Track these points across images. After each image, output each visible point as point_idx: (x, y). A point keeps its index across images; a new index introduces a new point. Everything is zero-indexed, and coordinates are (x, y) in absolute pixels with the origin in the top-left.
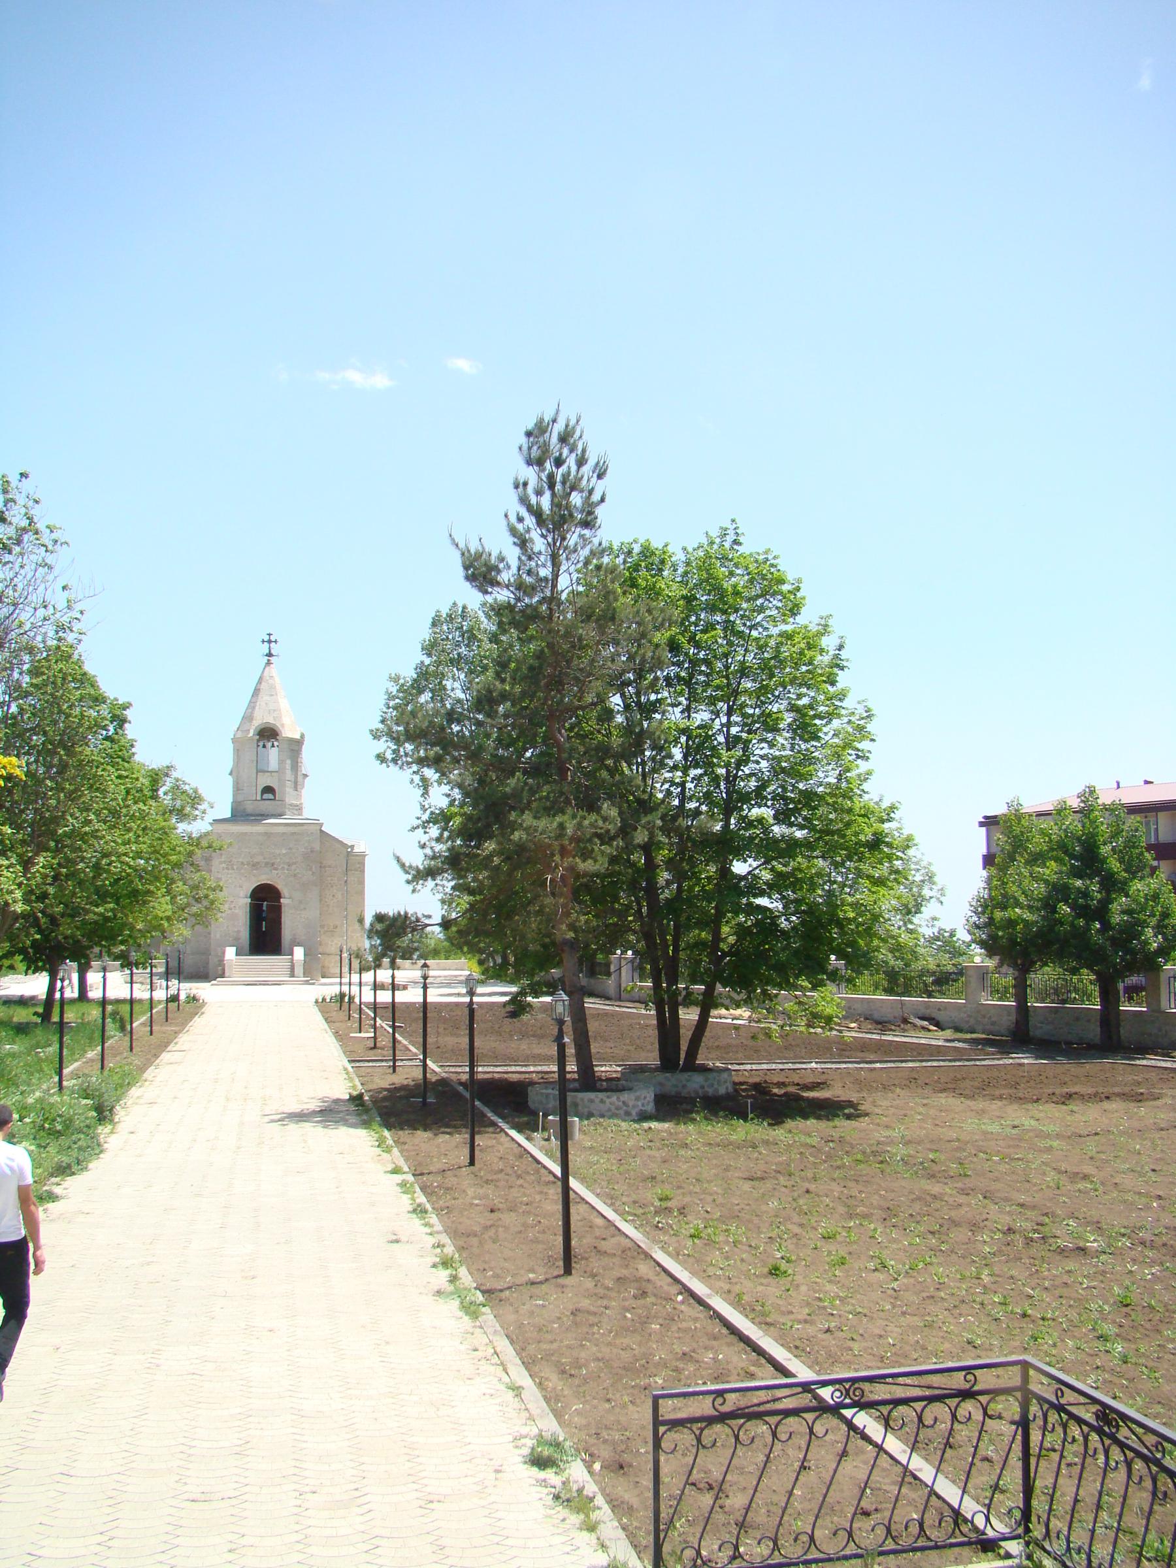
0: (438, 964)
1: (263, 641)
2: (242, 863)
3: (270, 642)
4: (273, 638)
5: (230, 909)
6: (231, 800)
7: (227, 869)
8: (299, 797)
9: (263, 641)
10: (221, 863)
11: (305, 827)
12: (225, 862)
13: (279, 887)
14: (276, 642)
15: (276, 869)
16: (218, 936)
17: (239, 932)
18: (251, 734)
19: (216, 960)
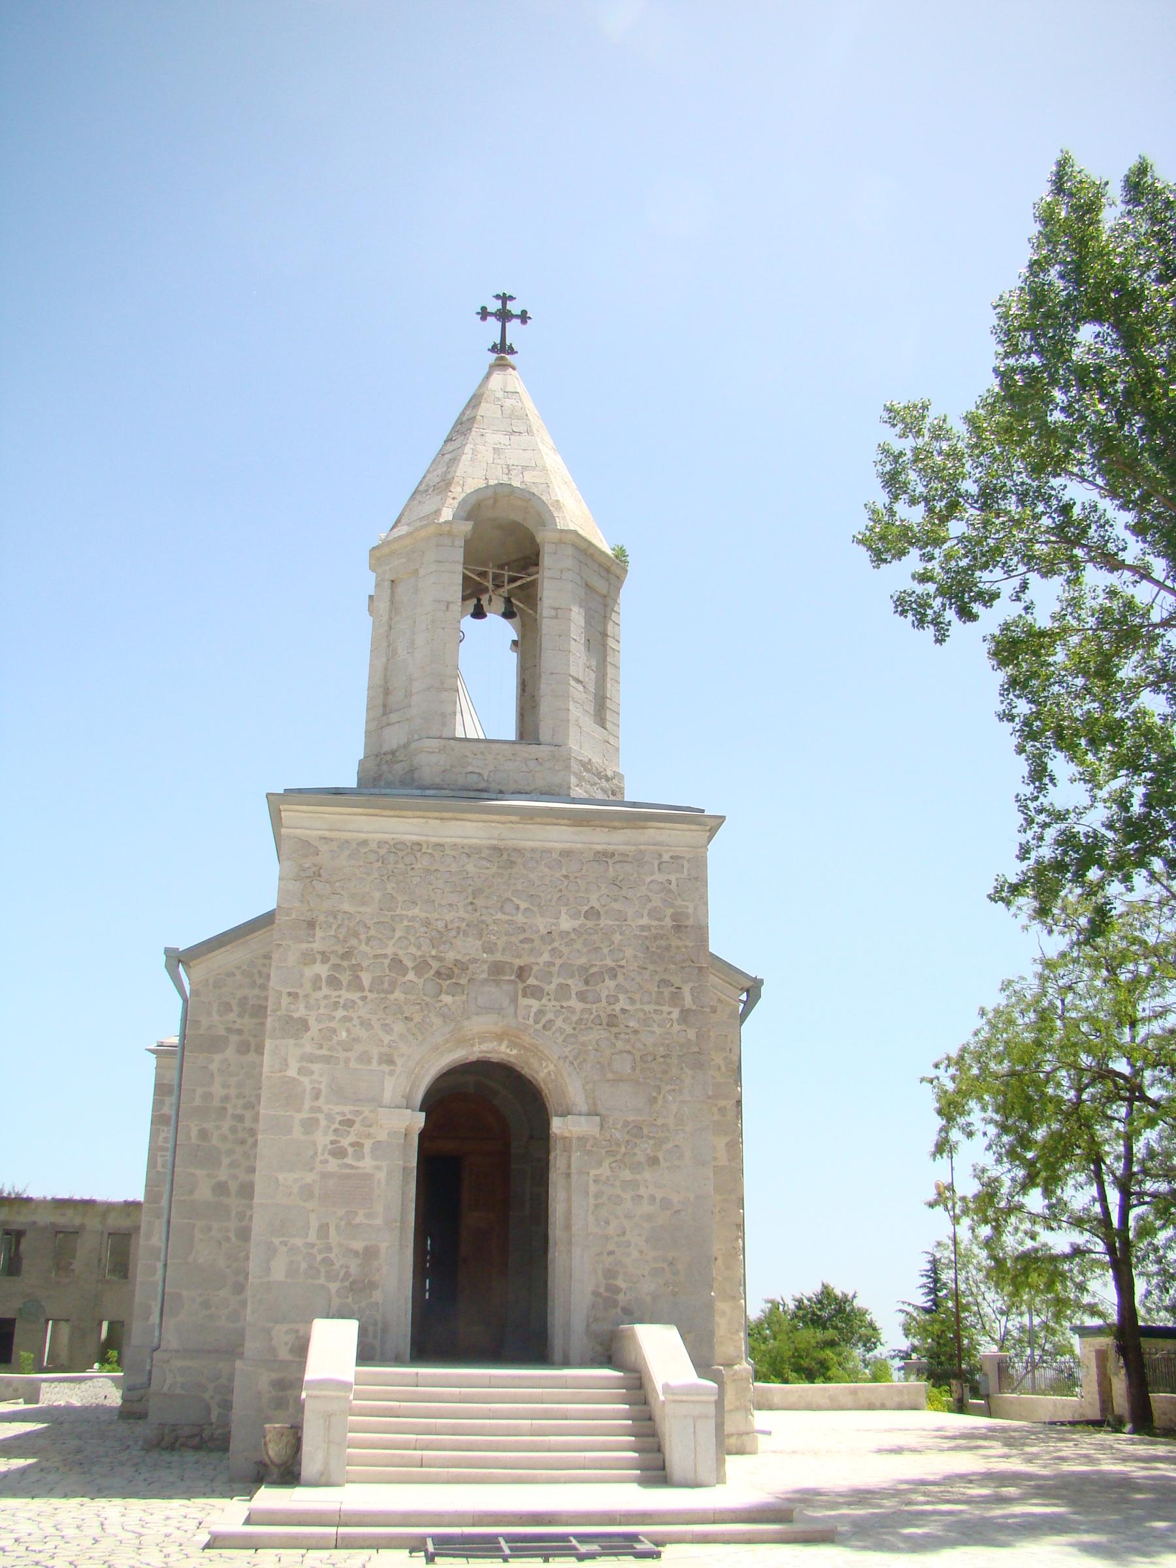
0: (854, 1392)
1: (484, 314)
2: (397, 963)
3: (504, 316)
4: (514, 307)
5: (339, 1153)
7: (333, 982)
8: (611, 749)
10: (308, 958)
11: (651, 833)
12: (325, 958)
14: (524, 317)
15: (535, 992)
16: (279, 1272)
17: (370, 1253)
18: (447, 514)
19: (264, 1379)
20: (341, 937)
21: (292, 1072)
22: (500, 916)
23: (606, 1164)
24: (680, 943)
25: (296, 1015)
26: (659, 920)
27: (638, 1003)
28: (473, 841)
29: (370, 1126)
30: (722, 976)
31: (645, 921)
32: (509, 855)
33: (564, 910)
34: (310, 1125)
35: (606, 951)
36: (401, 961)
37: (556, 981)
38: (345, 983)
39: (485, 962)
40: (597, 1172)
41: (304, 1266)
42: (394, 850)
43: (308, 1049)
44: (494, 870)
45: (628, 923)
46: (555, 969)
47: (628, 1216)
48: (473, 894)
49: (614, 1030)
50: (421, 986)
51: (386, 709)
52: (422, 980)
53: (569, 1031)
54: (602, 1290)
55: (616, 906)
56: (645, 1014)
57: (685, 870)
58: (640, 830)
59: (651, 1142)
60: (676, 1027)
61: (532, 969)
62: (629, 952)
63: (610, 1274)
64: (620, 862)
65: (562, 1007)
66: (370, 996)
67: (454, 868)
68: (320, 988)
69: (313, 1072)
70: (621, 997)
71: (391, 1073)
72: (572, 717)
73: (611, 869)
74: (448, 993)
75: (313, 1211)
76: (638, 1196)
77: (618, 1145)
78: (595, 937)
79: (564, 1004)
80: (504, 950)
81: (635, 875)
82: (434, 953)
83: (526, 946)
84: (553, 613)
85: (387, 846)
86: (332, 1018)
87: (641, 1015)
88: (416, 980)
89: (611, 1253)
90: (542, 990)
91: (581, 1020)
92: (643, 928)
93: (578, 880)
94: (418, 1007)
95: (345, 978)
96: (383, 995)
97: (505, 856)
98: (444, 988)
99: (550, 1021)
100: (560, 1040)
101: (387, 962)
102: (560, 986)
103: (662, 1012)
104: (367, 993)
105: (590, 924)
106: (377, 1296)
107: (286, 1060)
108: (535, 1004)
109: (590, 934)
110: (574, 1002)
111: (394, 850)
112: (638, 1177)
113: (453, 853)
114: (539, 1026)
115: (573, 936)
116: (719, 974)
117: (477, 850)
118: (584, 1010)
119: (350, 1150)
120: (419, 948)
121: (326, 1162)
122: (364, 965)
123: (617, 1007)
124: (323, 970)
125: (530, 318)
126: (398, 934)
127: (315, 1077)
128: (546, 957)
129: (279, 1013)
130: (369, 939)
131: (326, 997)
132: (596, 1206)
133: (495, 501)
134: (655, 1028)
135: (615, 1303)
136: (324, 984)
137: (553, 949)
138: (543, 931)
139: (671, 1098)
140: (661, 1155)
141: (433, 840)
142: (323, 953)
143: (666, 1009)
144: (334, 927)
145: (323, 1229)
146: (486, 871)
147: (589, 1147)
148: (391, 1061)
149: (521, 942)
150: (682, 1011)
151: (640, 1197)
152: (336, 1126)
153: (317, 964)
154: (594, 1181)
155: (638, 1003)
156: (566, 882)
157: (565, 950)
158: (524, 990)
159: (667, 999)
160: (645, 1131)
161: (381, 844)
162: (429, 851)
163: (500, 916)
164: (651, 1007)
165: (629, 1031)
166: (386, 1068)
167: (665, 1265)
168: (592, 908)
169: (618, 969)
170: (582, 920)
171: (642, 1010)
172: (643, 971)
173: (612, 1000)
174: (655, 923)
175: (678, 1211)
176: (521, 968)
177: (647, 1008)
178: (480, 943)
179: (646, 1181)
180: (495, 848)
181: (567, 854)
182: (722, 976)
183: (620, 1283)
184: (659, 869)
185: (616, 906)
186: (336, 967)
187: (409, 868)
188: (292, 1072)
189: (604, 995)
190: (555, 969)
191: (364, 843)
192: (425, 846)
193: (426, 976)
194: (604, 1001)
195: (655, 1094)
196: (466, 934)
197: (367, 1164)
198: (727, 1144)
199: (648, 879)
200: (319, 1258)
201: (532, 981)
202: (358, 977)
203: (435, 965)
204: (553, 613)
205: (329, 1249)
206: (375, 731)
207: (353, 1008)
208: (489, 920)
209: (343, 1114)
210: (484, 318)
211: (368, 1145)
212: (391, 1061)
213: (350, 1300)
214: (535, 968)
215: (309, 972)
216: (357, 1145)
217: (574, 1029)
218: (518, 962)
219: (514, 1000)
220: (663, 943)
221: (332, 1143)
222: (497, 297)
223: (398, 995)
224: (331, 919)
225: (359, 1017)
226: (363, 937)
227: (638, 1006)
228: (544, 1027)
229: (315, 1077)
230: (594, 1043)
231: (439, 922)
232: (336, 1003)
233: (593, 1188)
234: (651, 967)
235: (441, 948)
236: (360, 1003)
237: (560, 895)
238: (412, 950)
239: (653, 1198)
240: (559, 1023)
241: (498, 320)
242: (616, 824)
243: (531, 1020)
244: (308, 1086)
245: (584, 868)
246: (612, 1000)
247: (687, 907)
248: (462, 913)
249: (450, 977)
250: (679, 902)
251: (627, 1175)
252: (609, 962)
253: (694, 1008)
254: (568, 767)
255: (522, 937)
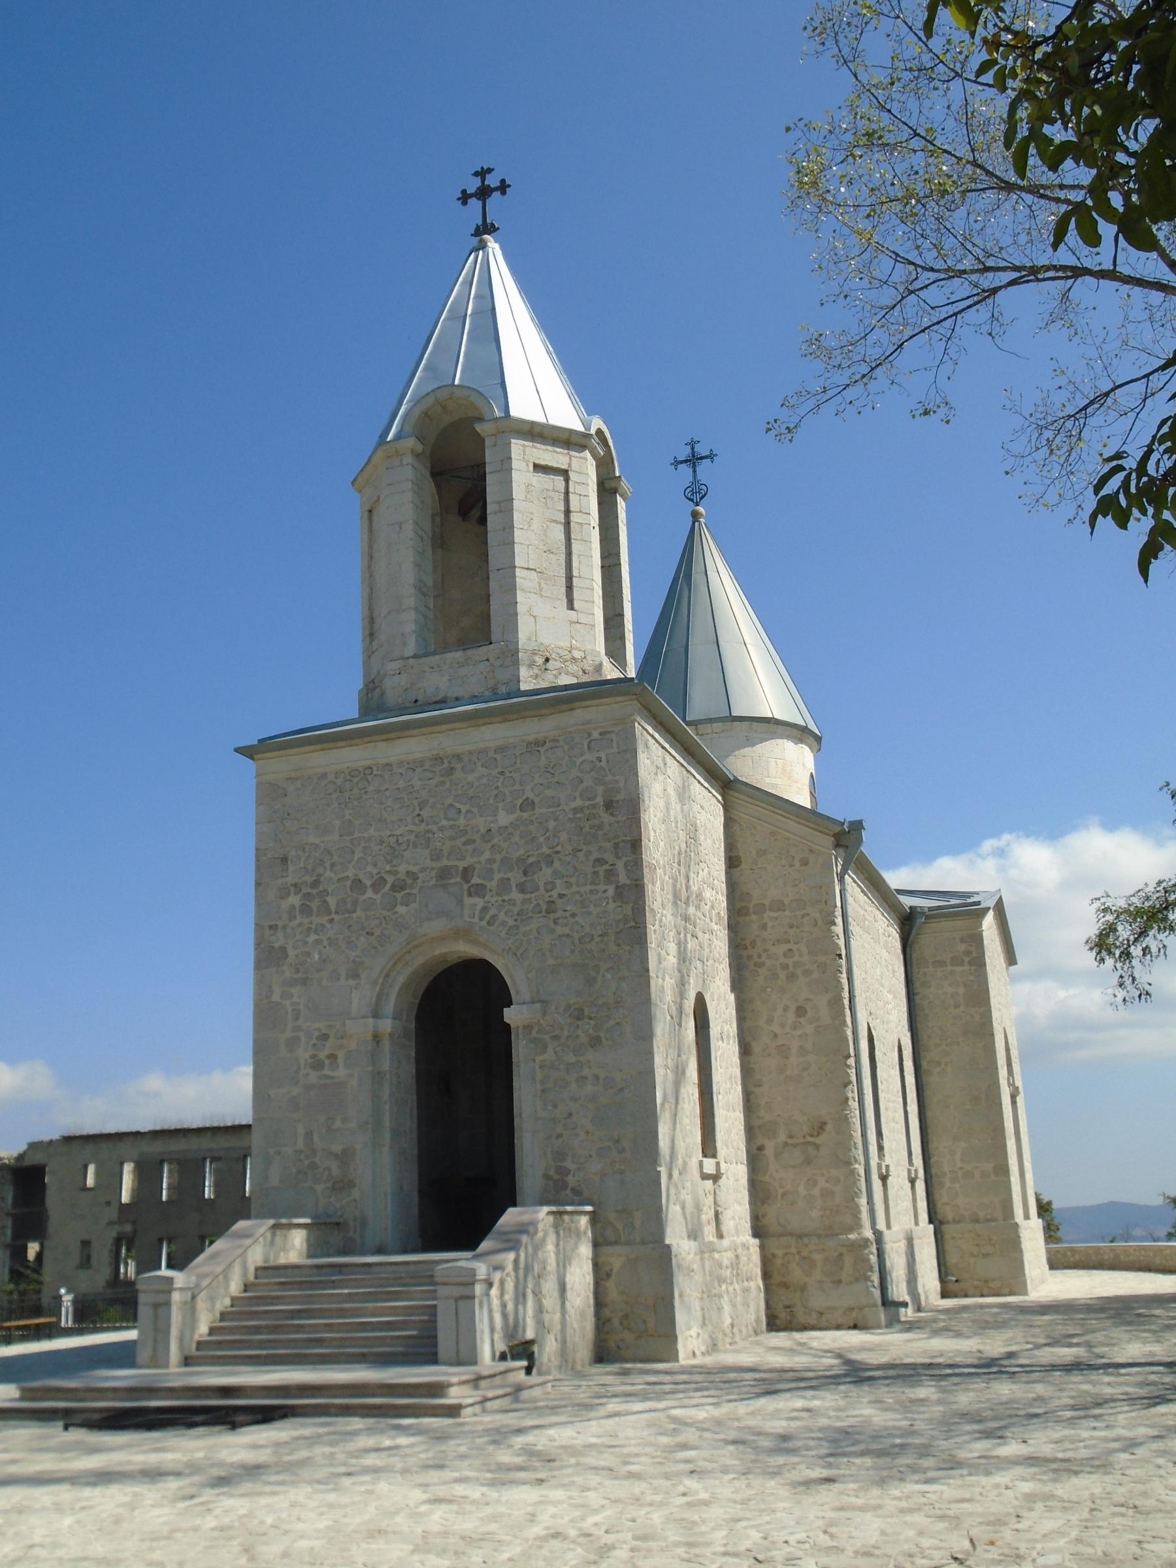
1: (465, 198)
2: (358, 884)
4: (492, 181)
5: (317, 1065)
6: (360, 684)
7: (306, 910)
9: (465, 198)
10: (284, 893)
13: (499, 963)
14: (503, 187)
15: (478, 891)
20: (310, 867)
21: (276, 997)
22: (444, 822)
23: (550, 1049)
24: (612, 819)
25: (277, 945)
26: (590, 799)
27: (574, 886)
28: (418, 755)
29: (342, 1038)
30: (812, 825)
31: (578, 803)
32: (449, 763)
33: (500, 805)
34: (292, 1044)
35: (542, 839)
36: (360, 881)
37: (497, 876)
38: (315, 909)
39: (433, 869)
40: (542, 1058)
41: (294, 1171)
42: (349, 778)
43: (288, 973)
44: (438, 779)
45: (561, 808)
46: (495, 866)
47: (575, 1100)
48: (419, 805)
49: (552, 916)
50: (378, 901)
51: (372, 635)
52: (379, 896)
53: (511, 922)
54: (552, 1173)
55: (549, 793)
56: (582, 896)
57: (615, 745)
58: (567, 713)
59: (593, 1022)
60: (612, 905)
61: (474, 869)
62: (564, 837)
63: (560, 1156)
64: (552, 748)
65: (504, 901)
66: (337, 918)
67: (401, 784)
68: (295, 917)
69: (292, 996)
70: (558, 882)
71: (356, 988)
72: (521, 609)
73: (543, 757)
74: (401, 904)
75: (299, 1121)
76: (582, 1077)
77: (562, 1029)
78: (532, 828)
79: (506, 898)
80: (449, 854)
81: (567, 758)
82: (388, 868)
83: (470, 848)
84: (496, 507)
85: (343, 775)
86: (306, 943)
87: (578, 897)
88: (375, 897)
89: (560, 1136)
90: (483, 886)
91: (522, 910)
92: (575, 810)
93: (513, 774)
94: (376, 922)
95: (315, 905)
96: (347, 915)
97: (446, 765)
98: (399, 900)
99: (493, 916)
100: (504, 933)
101: (348, 883)
102: (501, 880)
103: (598, 892)
104: (334, 916)
105: (525, 815)
106: (356, 1193)
107: (270, 986)
108: (479, 902)
109: (526, 825)
110: (515, 895)
111: (349, 778)
112: (582, 1059)
113: (400, 770)
114: (484, 923)
115: (510, 830)
116: (807, 823)
117: (421, 763)
118: (524, 901)
119: (327, 1062)
120: (375, 865)
121: (308, 1074)
122: (330, 890)
123: (555, 893)
124: (295, 900)
125: (509, 186)
126: (356, 858)
127: (295, 999)
128: (487, 855)
129: (263, 946)
130: (332, 865)
131: (300, 925)
132: (543, 1091)
133: (444, 408)
134: (592, 908)
135: (565, 1185)
136: (297, 912)
137: (493, 846)
138: (483, 830)
139: (609, 976)
140: (602, 1034)
141: (383, 761)
142: (295, 885)
143: (602, 887)
144: (303, 859)
145: (309, 1135)
146: (428, 782)
147: (534, 1034)
148: (356, 976)
149: (464, 844)
150: (617, 887)
151: (586, 1078)
152: (315, 1041)
153: (292, 895)
154: (540, 1067)
155: (574, 886)
156: (502, 778)
157: (504, 845)
158: (469, 890)
159: (602, 878)
160: (586, 1013)
161: (337, 774)
162: (379, 773)
163: (444, 822)
164: (589, 887)
165: (568, 914)
166: (352, 982)
167: (611, 1144)
168: (527, 799)
169: (554, 855)
170: (518, 813)
171: (578, 892)
172: (580, 854)
173: (550, 886)
174: (587, 803)
175: (622, 1089)
176: (465, 869)
177: (582, 890)
178: (427, 852)
179: (589, 1061)
180: (438, 759)
181: (501, 749)
182: (812, 825)
183: (569, 1164)
184: (589, 748)
185: (549, 793)
186: (307, 896)
187: (363, 791)
188: (276, 997)
189: (541, 885)
190: (495, 866)
191: (324, 776)
192: (375, 769)
193: (383, 891)
194: (541, 885)
195: (593, 974)
196: (415, 846)
197: (341, 1073)
198: (829, 1002)
199: (578, 762)
200: (306, 1162)
201: (475, 880)
202: (326, 902)
203: (390, 880)
204: (496, 507)
205: (314, 1152)
206: (367, 662)
207: (322, 931)
208: (434, 828)
209: (319, 1030)
210: (465, 203)
211: (341, 1055)
212: (356, 976)
213: (333, 1197)
214: (477, 866)
215: (285, 904)
216: (333, 1057)
217: (516, 920)
218: (462, 864)
219: (460, 902)
220: (596, 822)
221: (311, 1057)
222: (476, 174)
223: (358, 909)
224: (300, 853)
225: (329, 939)
226: (328, 865)
227: (574, 889)
228: (488, 923)
229: (295, 999)
230: (535, 931)
231: (391, 839)
232: (309, 929)
233: (539, 1075)
234: (585, 848)
235: (394, 863)
236: (328, 926)
237: (496, 792)
238: (370, 868)
239: (597, 1077)
240: (502, 916)
241: (478, 199)
242: (544, 711)
243: (476, 920)
244: (290, 1009)
245: (518, 761)
246: (550, 886)
247: (617, 782)
248: (411, 827)
249: (402, 889)
250: (609, 778)
251: (571, 1058)
252: (545, 850)
253: (628, 882)
254: (516, 663)
255: (463, 839)
